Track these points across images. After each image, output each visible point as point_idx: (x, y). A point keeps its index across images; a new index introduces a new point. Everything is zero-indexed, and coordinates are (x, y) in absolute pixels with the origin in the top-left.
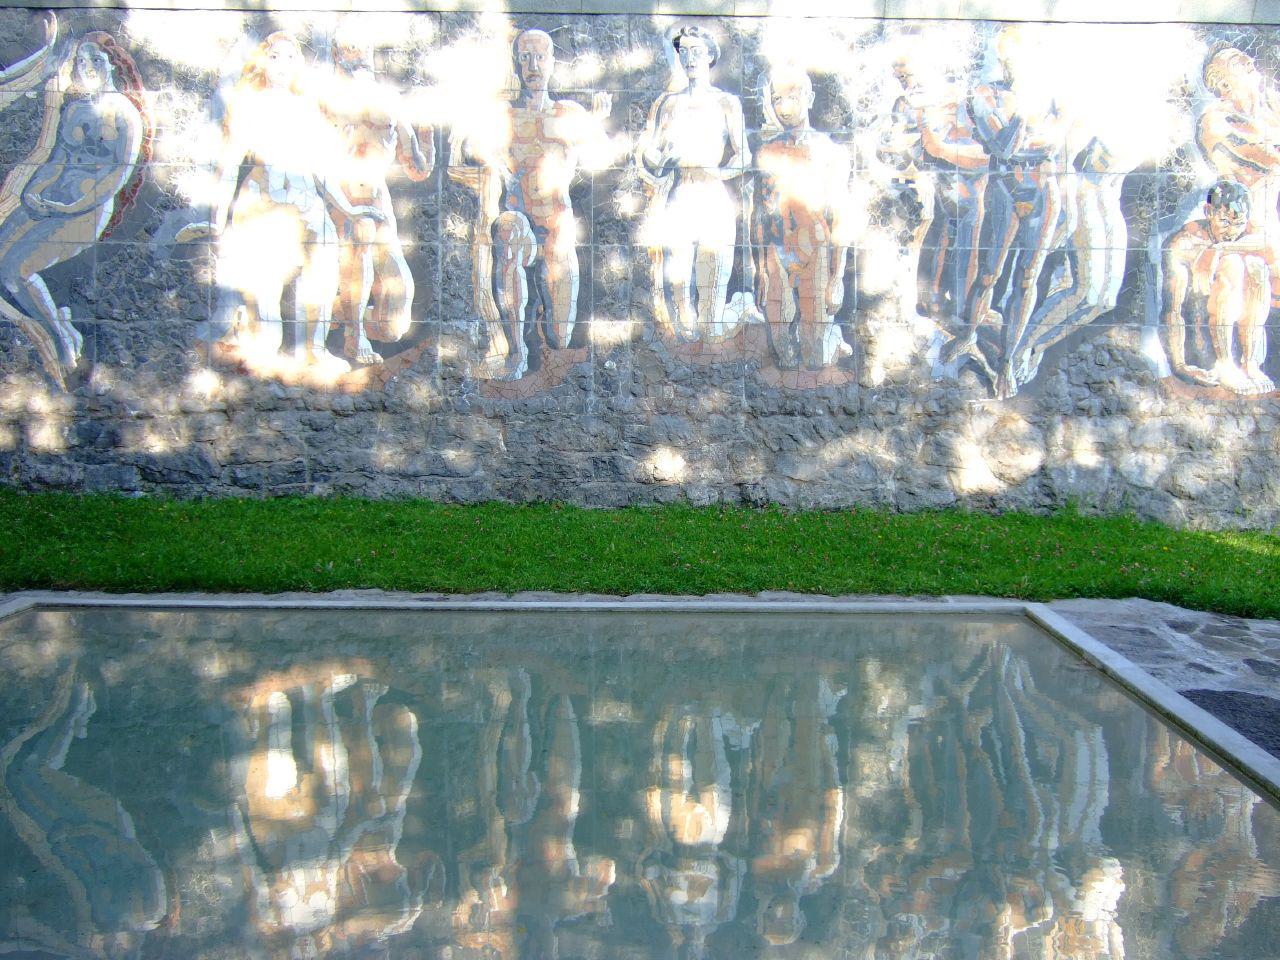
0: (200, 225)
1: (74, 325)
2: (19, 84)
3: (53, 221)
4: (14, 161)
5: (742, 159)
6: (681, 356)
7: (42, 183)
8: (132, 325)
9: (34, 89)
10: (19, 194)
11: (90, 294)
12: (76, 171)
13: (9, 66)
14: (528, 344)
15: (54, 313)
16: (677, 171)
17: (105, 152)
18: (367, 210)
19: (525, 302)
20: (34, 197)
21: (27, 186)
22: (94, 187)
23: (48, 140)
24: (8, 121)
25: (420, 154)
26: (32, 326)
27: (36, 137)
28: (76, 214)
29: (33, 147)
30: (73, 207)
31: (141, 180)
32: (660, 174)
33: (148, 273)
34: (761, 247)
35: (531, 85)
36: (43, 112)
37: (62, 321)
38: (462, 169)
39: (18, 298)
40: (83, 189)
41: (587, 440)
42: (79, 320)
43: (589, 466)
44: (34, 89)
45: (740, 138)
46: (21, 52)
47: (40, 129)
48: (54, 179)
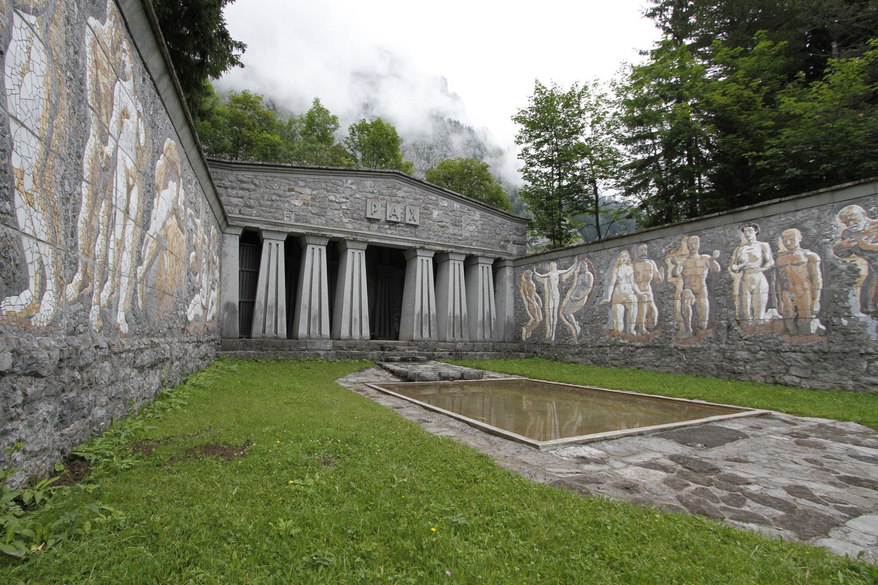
5: (771, 263)
23: (575, 284)
26: (571, 326)
34: (779, 293)
43: (713, 366)
45: (769, 255)
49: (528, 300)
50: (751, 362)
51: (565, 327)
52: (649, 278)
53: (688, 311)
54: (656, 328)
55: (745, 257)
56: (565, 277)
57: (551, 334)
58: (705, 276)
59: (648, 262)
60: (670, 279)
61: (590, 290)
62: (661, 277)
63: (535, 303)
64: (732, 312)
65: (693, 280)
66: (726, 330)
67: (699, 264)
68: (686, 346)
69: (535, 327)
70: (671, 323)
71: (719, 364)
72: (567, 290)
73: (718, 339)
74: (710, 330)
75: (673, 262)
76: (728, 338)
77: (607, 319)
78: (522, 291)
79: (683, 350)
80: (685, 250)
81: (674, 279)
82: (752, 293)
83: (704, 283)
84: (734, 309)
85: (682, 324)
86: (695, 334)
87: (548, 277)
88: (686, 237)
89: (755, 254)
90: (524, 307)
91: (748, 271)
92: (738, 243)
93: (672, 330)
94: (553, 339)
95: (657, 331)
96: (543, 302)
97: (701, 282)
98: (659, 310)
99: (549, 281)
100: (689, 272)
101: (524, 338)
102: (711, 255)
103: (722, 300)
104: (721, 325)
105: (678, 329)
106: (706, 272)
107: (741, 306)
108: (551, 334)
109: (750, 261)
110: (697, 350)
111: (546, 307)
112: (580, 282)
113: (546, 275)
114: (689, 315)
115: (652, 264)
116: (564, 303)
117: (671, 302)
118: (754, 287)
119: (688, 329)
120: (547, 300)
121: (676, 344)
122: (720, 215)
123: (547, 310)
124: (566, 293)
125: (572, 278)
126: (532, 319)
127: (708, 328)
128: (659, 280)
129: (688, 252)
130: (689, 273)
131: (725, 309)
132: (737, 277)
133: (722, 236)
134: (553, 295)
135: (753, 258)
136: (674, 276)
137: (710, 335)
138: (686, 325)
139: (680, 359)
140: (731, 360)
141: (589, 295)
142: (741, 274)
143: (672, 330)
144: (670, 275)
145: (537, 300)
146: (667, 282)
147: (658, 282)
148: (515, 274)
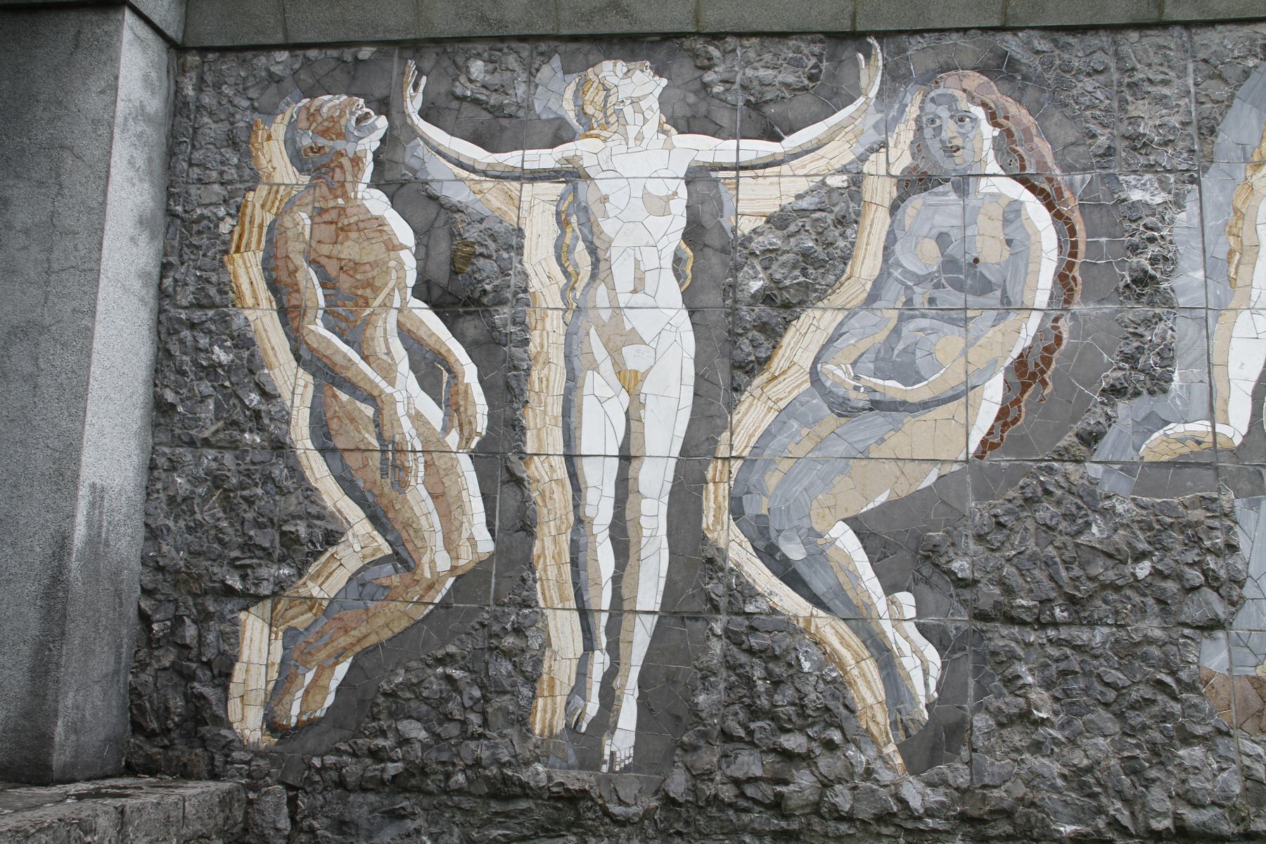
0: (1190, 427)
1: (923, 630)
2: (811, 164)
3: (877, 418)
4: (801, 303)
7: (851, 345)
8: (1051, 633)
9: (842, 171)
10: (807, 365)
11: (961, 566)
12: (924, 323)
13: (791, 131)
15: (881, 604)
17: (985, 287)
20: (838, 373)
21: (824, 348)
22: (965, 353)
23: (867, 265)
24: (792, 228)
26: (831, 630)
27: (845, 259)
28: (925, 406)
29: (838, 278)
30: (918, 392)
31: (1059, 339)
33: (1088, 525)
36: (858, 214)
37: (898, 621)
39: (803, 571)
40: (940, 356)
42: (930, 620)
44: (842, 171)
46: (815, 109)
47: (853, 244)
48: (882, 336)
49: (326, 373)
51: (763, 651)
56: (754, 202)
57: (586, 687)
61: (1034, 321)
63: (407, 395)
69: (389, 619)
72: (783, 306)
77: (1230, 587)
78: (247, 271)
87: (571, 175)
90: (265, 416)
94: (622, 742)
96: (507, 389)
99: (579, 219)
101: (247, 721)
108: (586, 687)
111: (542, 431)
112: (921, 257)
113: (545, 158)
116: (751, 418)
120: (547, 381)
123: (545, 472)
124: (773, 333)
125: (836, 212)
126: (361, 540)
134: (620, 338)
141: (1025, 373)
145: (431, 369)
148: (178, 107)
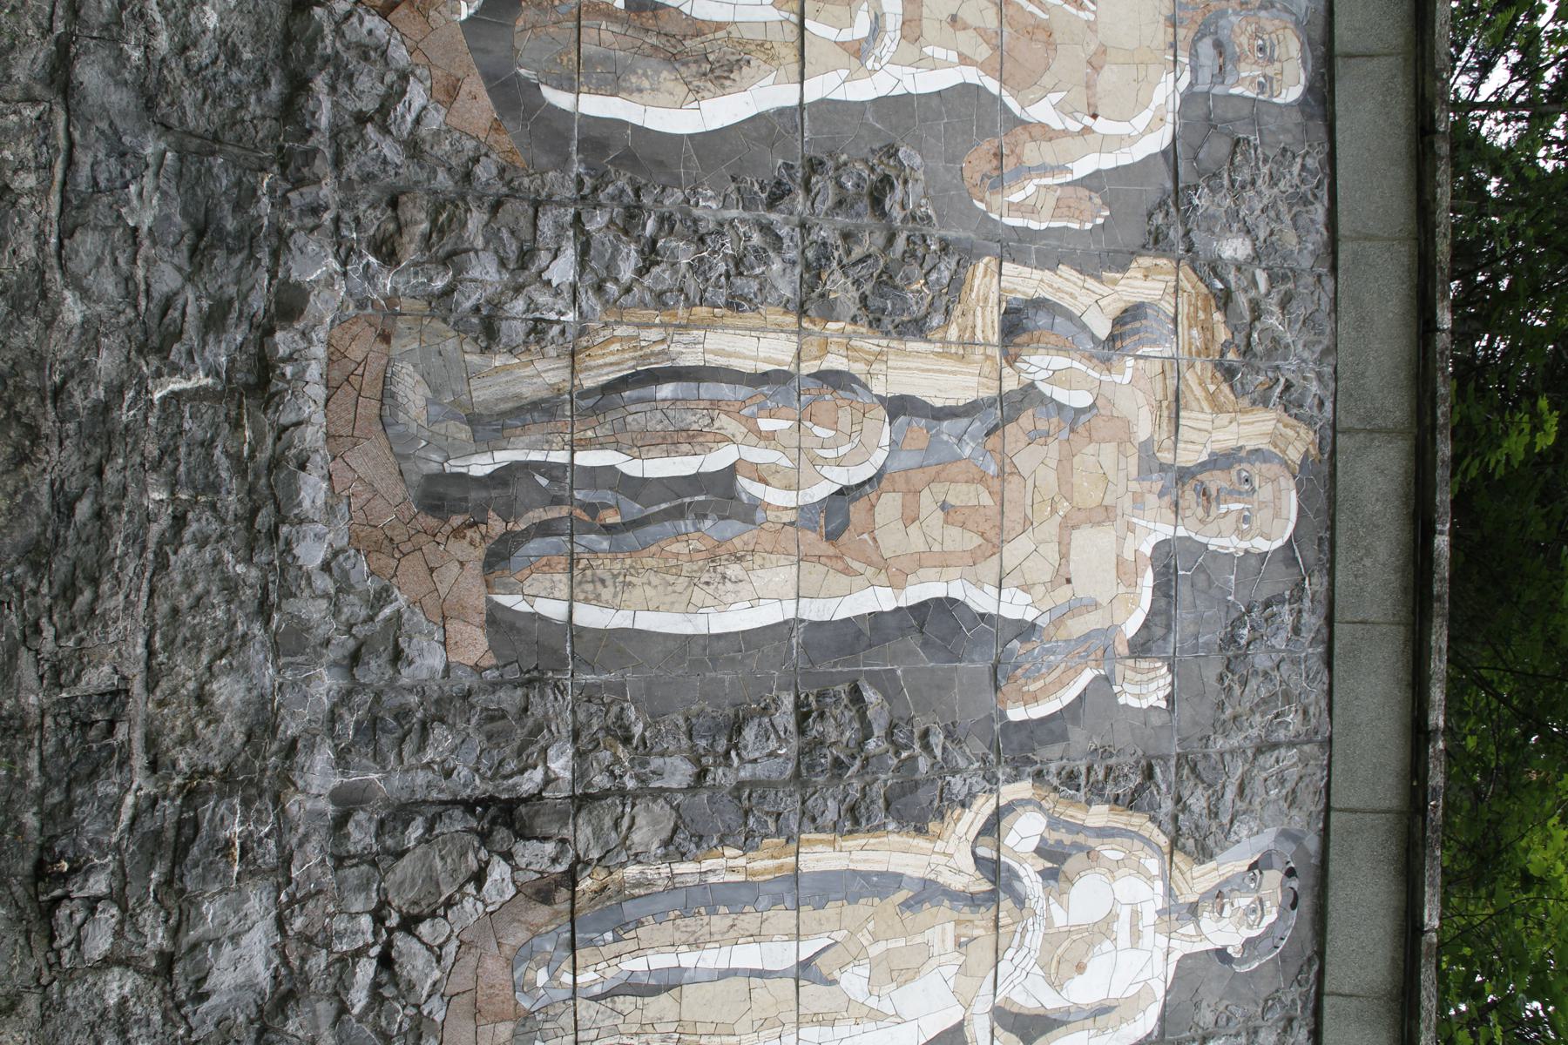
6: (470, 960)
14: (503, 477)
16: (992, 898)
18: (892, 23)
19: (632, 467)
25: (1030, 188)
32: (983, 852)
35: (1190, 497)
38: (993, 298)
41: (186, 670)
43: (97, 678)
50: (174, 1009)
52: (1028, 82)
53: (678, 439)
54: (512, 95)
55: (1088, 896)
58: (981, 600)
59: (1166, 91)
60: (992, 286)
62: (1023, 204)
64: (647, 830)
65: (961, 494)
66: (481, 787)
67: (1093, 551)
68: (309, 406)
70: (562, 270)
71: (130, 733)
73: (382, 727)
74: (474, 645)
75: (1129, 318)
76: (401, 813)
79: (259, 382)
80: (1211, 430)
81: (987, 323)
82: (804, 970)
83: (917, 593)
84: (672, 849)
85: (543, 374)
86: (442, 498)
88: (1299, 443)
89: (1098, 965)
91: (983, 918)
92: (1192, 841)
93: (485, 273)
95: (477, 107)
97: (944, 562)
98: (708, 143)
100: (1035, 462)
102: (1141, 647)
103: (765, 755)
104: (531, 748)
105: (488, 330)
106: (1016, 606)
107: (707, 898)
109: (1053, 938)
110: (266, 520)
114: (639, 445)
115: (1141, 132)
117: (783, 278)
118: (853, 981)
119: (490, 426)
121: (322, 307)
122: (1419, 733)
127: (498, 622)
128: (998, 182)
129: (1190, 456)
130: (1026, 459)
131: (678, 772)
132: (947, 853)
133: (1256, 727)
135: (1066, 957)
136: (1017, 323)
137: (428, 660)
138: (542, 409)
139: (157, 339)
140: (175, 850)
142: (964, 877)
143: (485, 273)
144: (1024, 281)
146: (968, 255)
147: (977, 163)
